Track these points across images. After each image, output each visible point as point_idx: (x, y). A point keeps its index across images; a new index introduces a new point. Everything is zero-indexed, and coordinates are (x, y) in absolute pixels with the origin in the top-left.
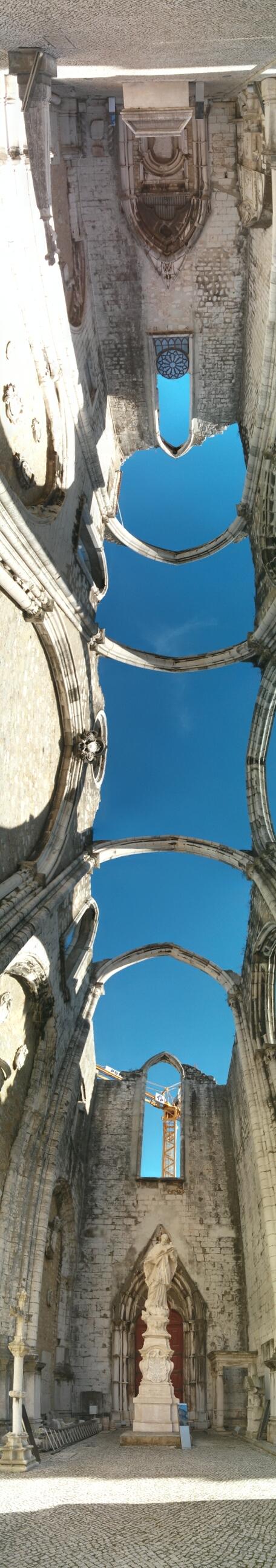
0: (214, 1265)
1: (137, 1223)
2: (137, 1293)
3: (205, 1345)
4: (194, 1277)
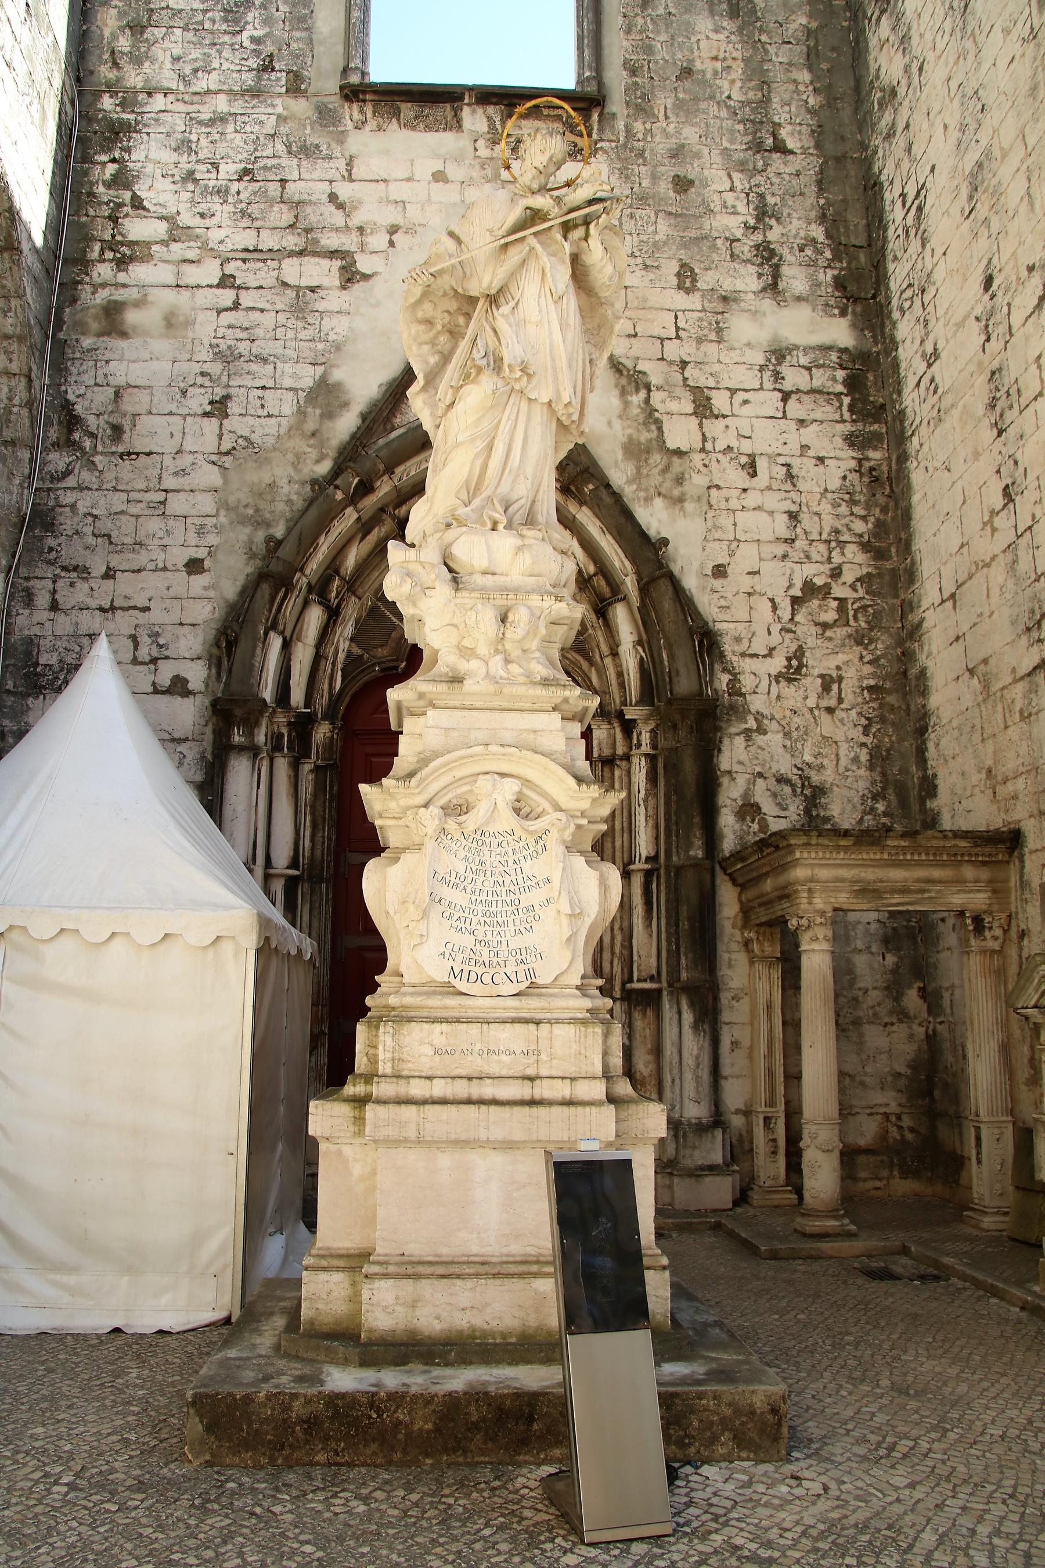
1: (350, 276)
4: (654, 518)
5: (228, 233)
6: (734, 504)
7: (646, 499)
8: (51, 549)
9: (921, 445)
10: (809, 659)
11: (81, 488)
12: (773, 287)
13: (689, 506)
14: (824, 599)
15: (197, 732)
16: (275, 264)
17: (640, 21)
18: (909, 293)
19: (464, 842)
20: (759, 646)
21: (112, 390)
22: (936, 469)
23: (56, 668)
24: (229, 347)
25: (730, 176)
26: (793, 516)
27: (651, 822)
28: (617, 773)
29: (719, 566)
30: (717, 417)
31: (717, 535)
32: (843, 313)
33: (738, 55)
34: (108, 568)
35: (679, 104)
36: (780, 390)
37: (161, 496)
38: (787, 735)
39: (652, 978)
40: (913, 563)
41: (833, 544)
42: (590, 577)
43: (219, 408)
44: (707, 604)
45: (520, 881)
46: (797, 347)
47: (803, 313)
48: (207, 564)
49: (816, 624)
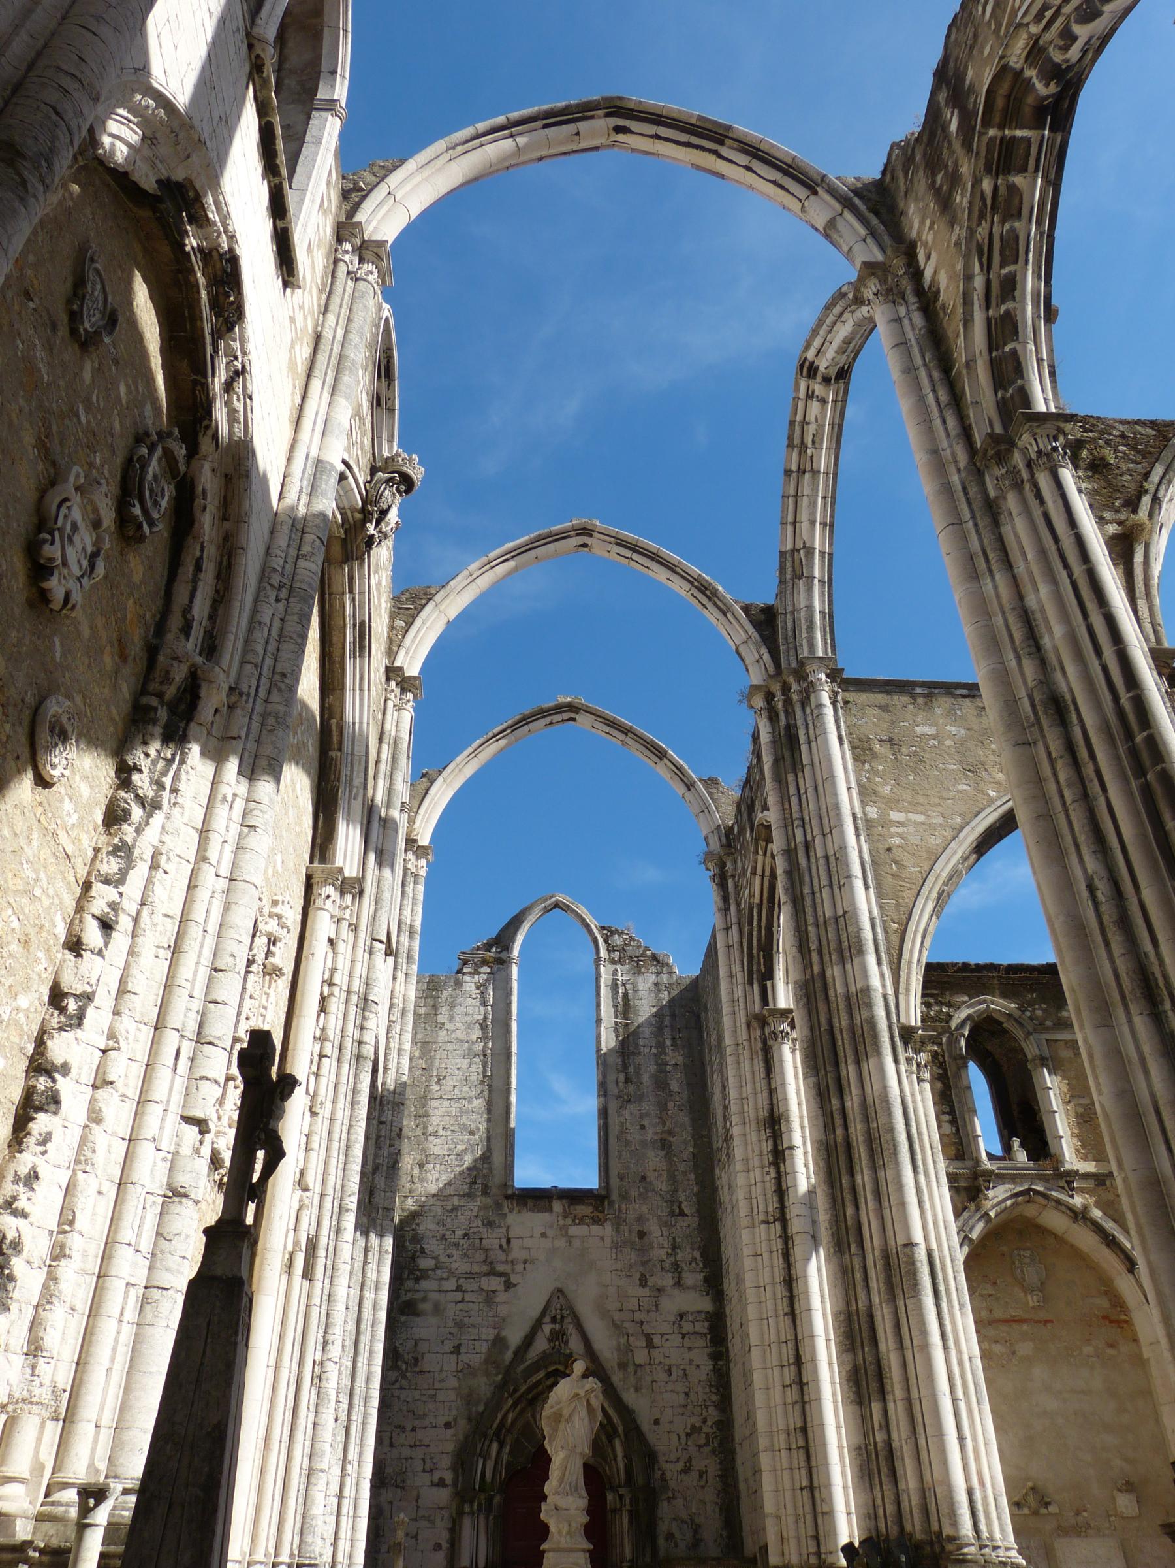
1: (509, 1285)
2: (509, 1431)
3: (653, 1539)
5: (460, 1266)
10: (693, 1463)
11: (401, 1388)
26: (687, 1394)
37: (433, 1392)
38: (685, 1499)
43: (457, 1350)
44: (651, 1438)
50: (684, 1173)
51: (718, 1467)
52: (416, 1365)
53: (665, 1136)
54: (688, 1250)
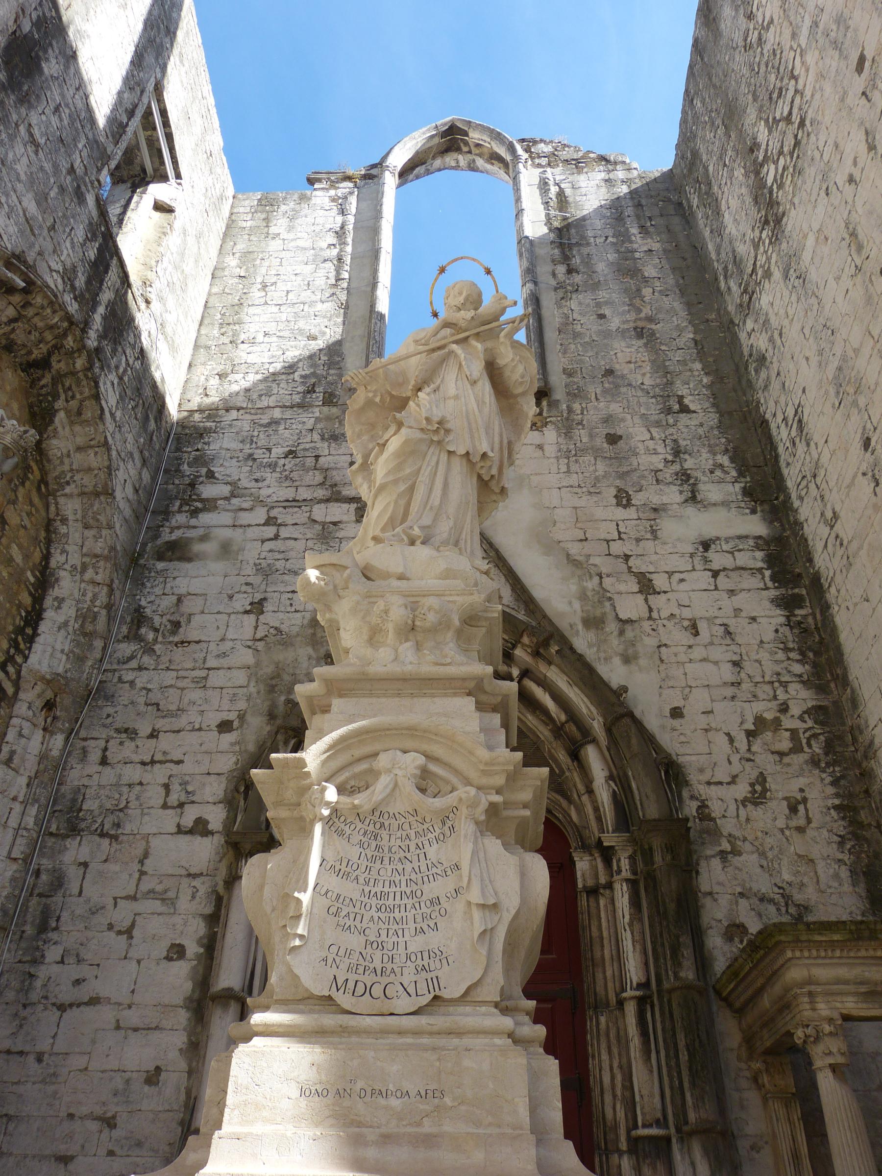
0: (694, 630)
3: (697, 935)
4: (614, 673)
5: (274, 490)
6: (683, 658)
7: (606, 659)
8: (108, 716)
9: (838, 591)
10: (771, 783)
11: (140, 668)
12: (693, 498)
13: (642, 662)
14: (776, 730)
15: (211, 867)
16: (308, 508)
17: (573, 346)
18: (804, 483)
19: (359, 825)
20: (722, 775)
21: (175, 597)
22: (856, 604)
23: (96, 813)
24: (269, 565)
25: (649, 431)
26: (736, 664)
27: (638, 947)
28: (602, 902)
29: (675, 708)
30: (659, 593)
31: (671, 684)
32: (753, 512)
33: (647, 359)
34: (154, 730)
35: (605, 391)
36: (710, 570)
37: (203, 673)
38: (763, 854)
39: (658, 1123)
40: (853, 691)
41: (776, 684)
42: (563, 724)
44: (668, 741)
45: (424, 868)
46: (718, 539)
47: (721, 514)
48: (236, 724)
49: (773, 753)
50: (684, 363)
51: (831, 790)
52: (174, 633)
53: (640, 324)
54: (705, 454)
